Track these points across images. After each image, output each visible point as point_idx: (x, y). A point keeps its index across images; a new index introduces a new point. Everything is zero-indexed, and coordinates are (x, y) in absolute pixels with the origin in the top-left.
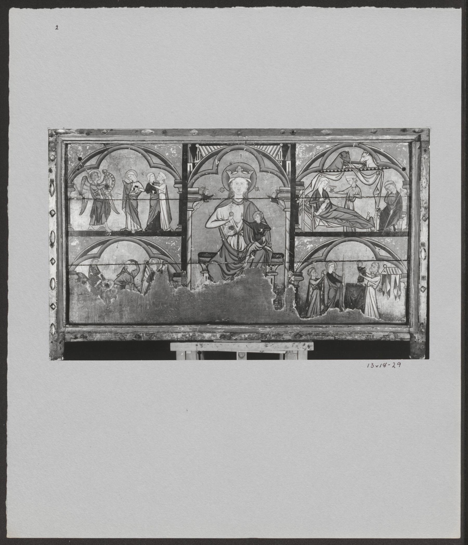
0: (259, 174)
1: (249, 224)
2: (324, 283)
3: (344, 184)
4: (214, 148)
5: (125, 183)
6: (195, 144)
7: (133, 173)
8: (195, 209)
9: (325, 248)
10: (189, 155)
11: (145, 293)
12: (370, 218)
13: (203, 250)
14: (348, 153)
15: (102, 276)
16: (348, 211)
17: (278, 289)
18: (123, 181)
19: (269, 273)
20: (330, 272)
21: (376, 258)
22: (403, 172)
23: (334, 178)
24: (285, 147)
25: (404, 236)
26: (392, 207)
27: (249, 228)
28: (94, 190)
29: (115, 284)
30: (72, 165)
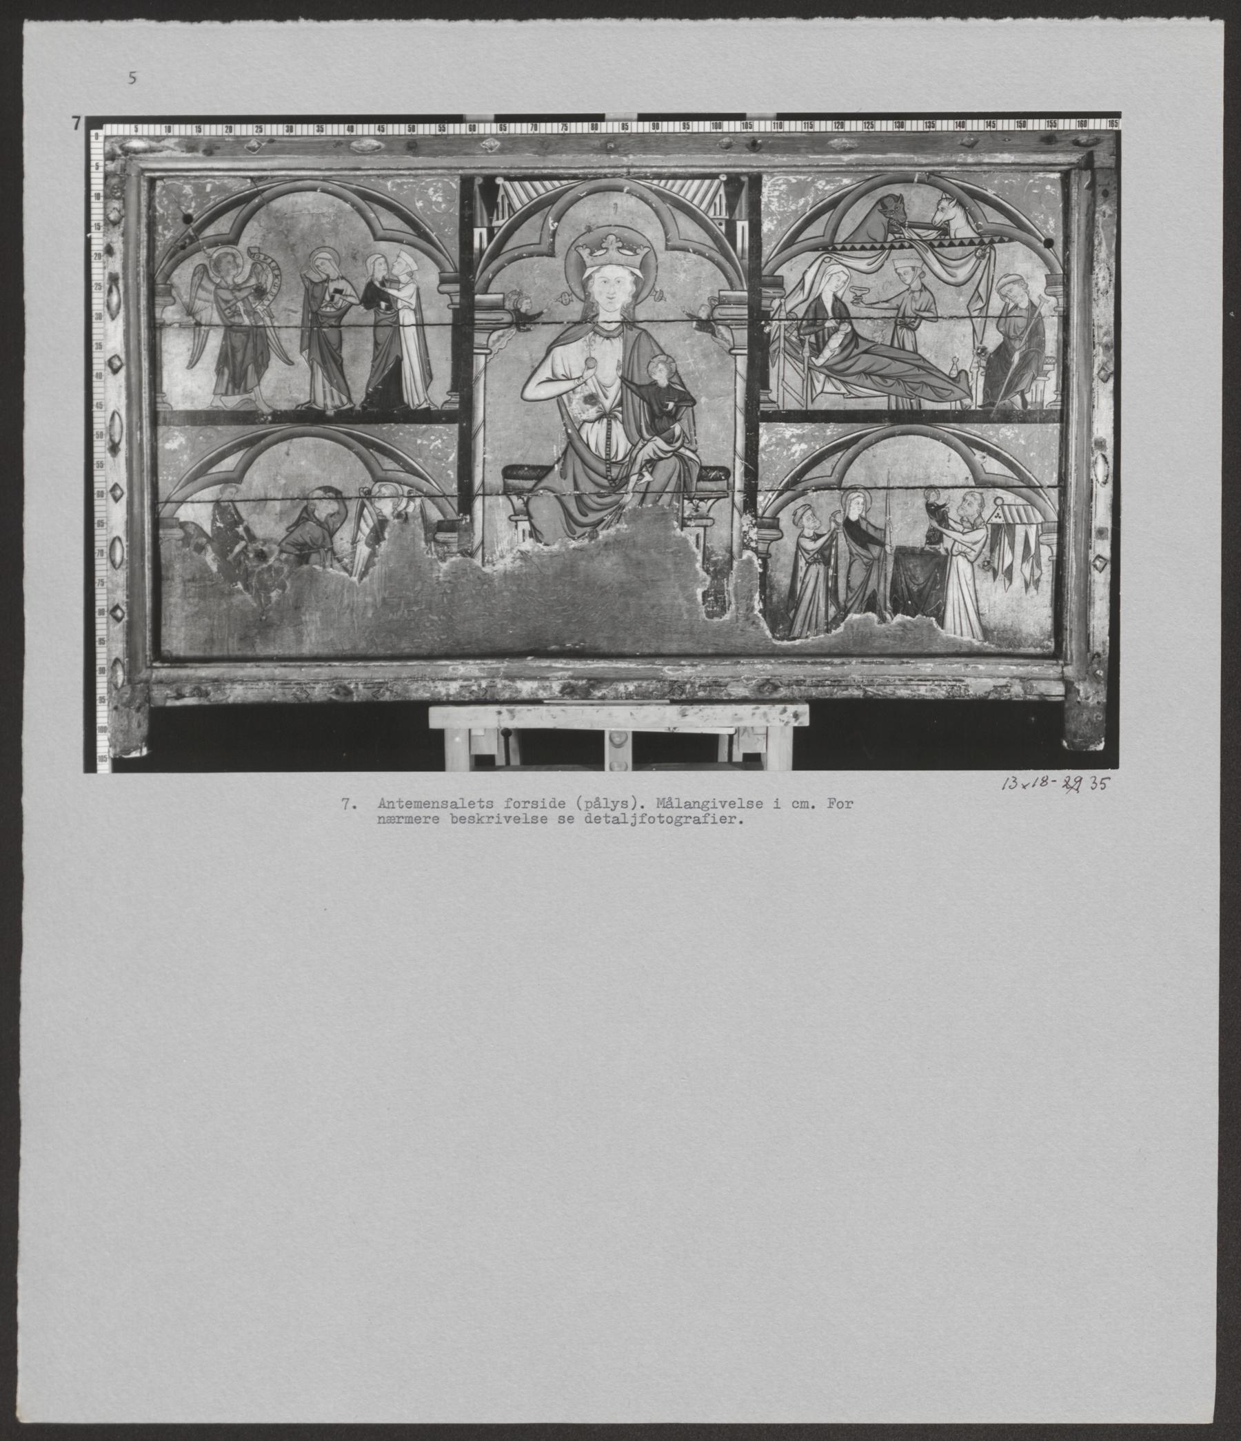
0: (664, 256)
1: (639, 390)
2: (837, 546)
3: (890, 283)
4: (544, 186)
6: (494, 177)
7: (329, 256)
8: (495, 349)
9: (839, 454)
10: (478, 206)
11: (363, 575)
12: (959, 373)
13: (516, 459)
14: (899, 199)
15: (247, 530)
16: (902, 354)
17: (715, 563)
18: (304, 278)
19: (690, 519)
20: (854, 517)
21: (975, 479)
22: (1047, 252)
23: (862, 265)
24: (733, 184)
25: (1049, 422)
26: (1017, 344)
27: (637, 399)
28: (227, 302)
29: (282, 552)
30: (166, 236)
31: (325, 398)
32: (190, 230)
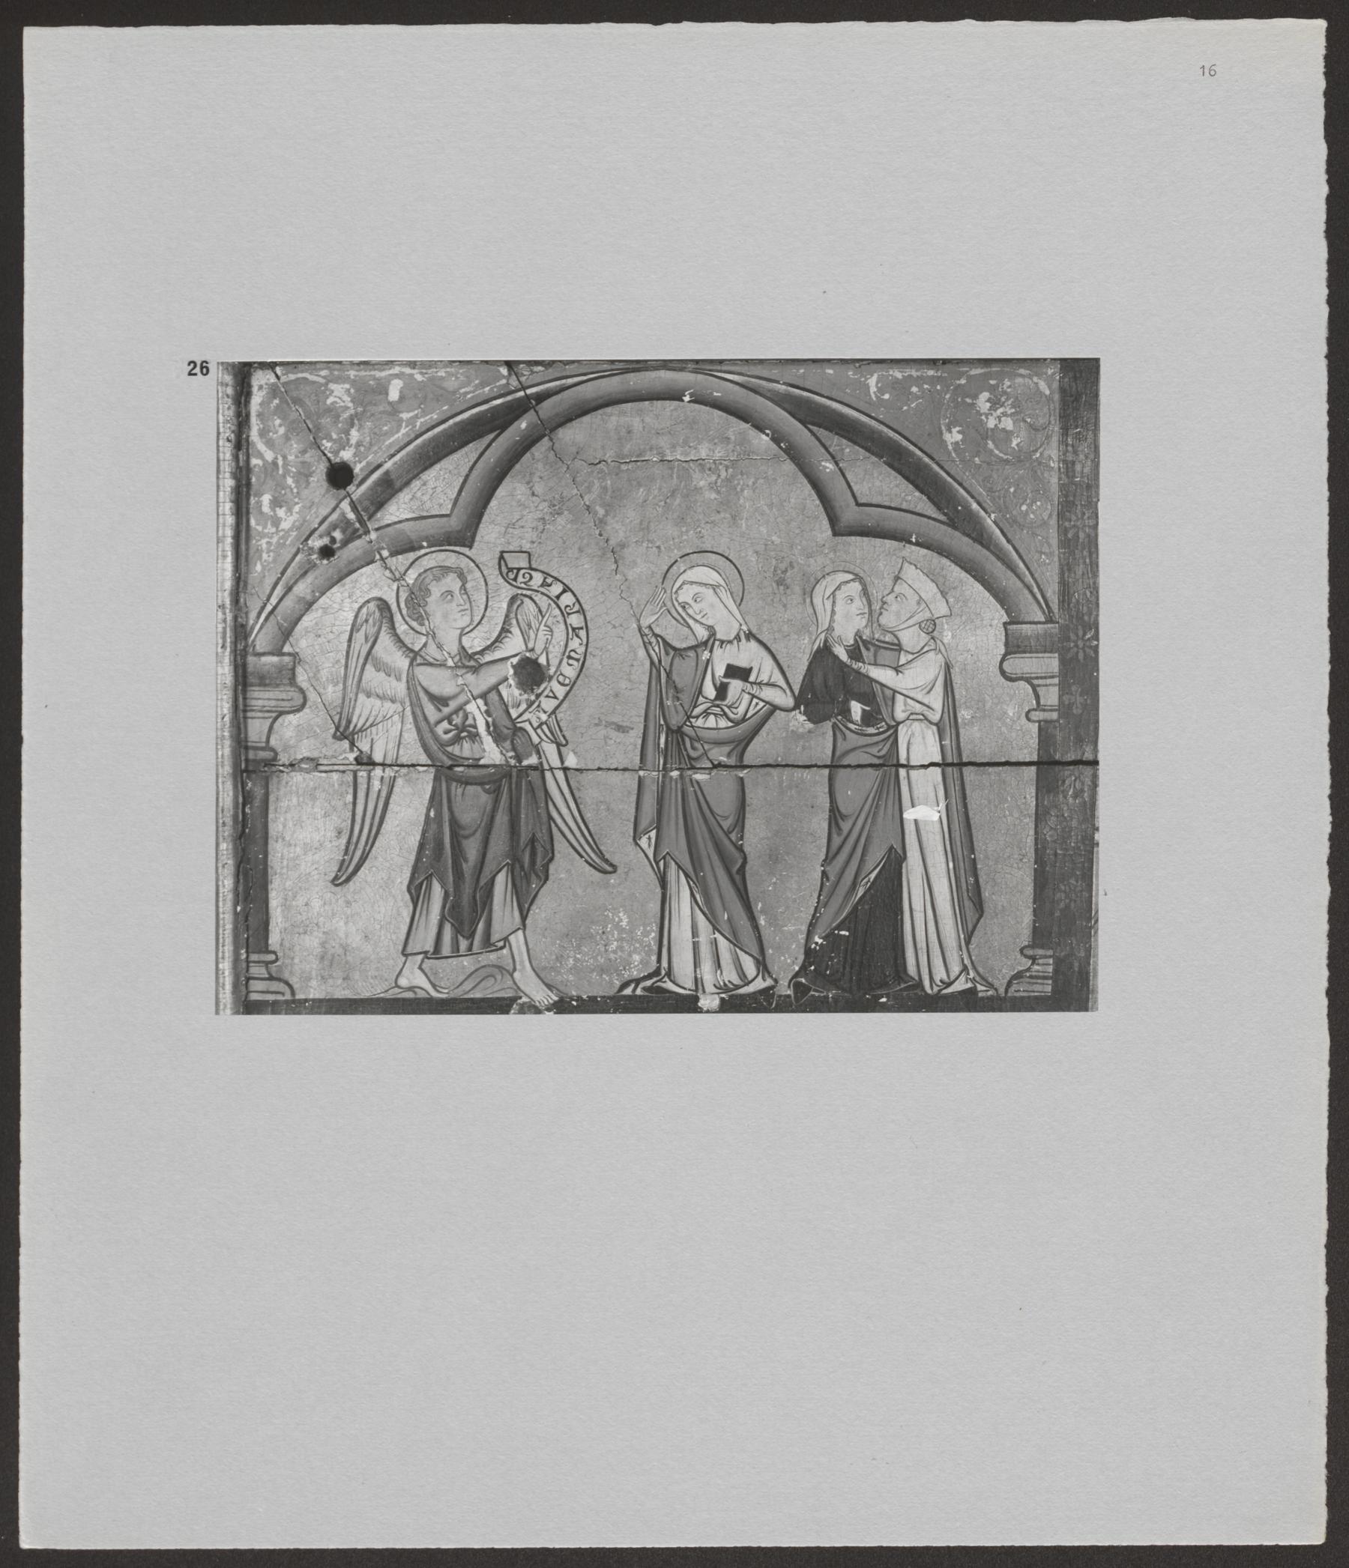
5: (657, 649)
7: (714, 577)
18: (648, 636)
28: (440, 701)
31: (696, 964)
32: (345, 506)
